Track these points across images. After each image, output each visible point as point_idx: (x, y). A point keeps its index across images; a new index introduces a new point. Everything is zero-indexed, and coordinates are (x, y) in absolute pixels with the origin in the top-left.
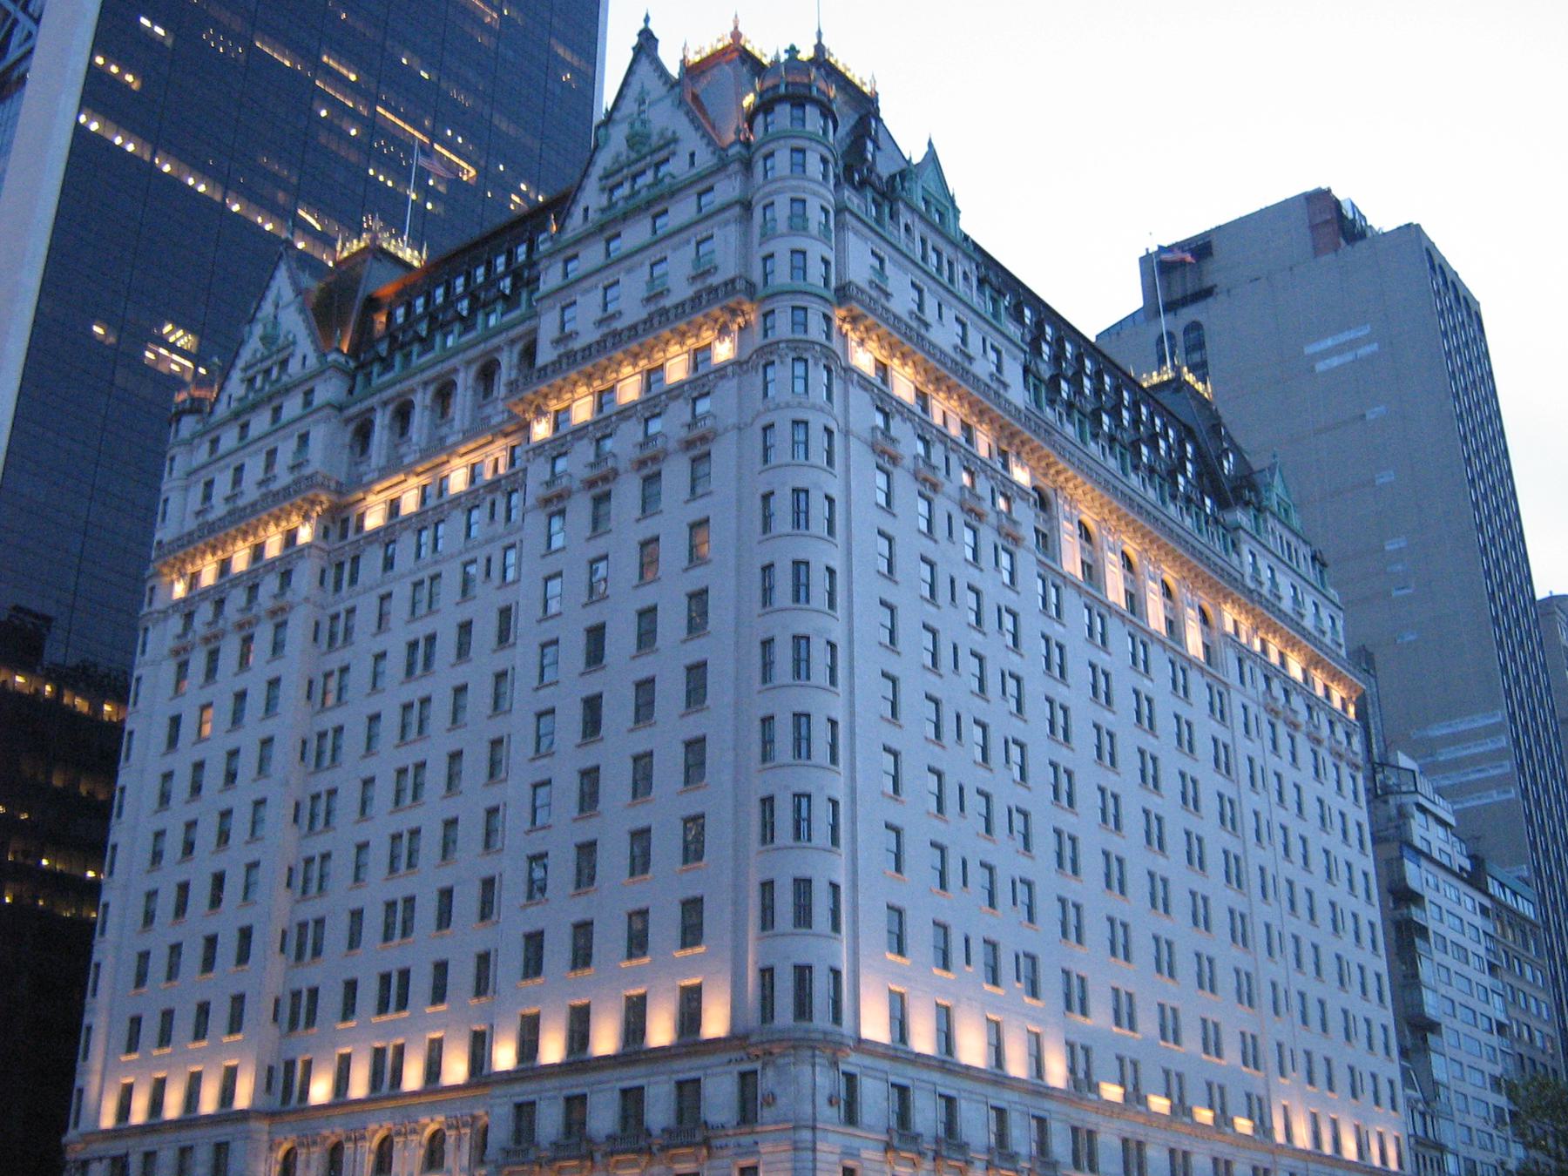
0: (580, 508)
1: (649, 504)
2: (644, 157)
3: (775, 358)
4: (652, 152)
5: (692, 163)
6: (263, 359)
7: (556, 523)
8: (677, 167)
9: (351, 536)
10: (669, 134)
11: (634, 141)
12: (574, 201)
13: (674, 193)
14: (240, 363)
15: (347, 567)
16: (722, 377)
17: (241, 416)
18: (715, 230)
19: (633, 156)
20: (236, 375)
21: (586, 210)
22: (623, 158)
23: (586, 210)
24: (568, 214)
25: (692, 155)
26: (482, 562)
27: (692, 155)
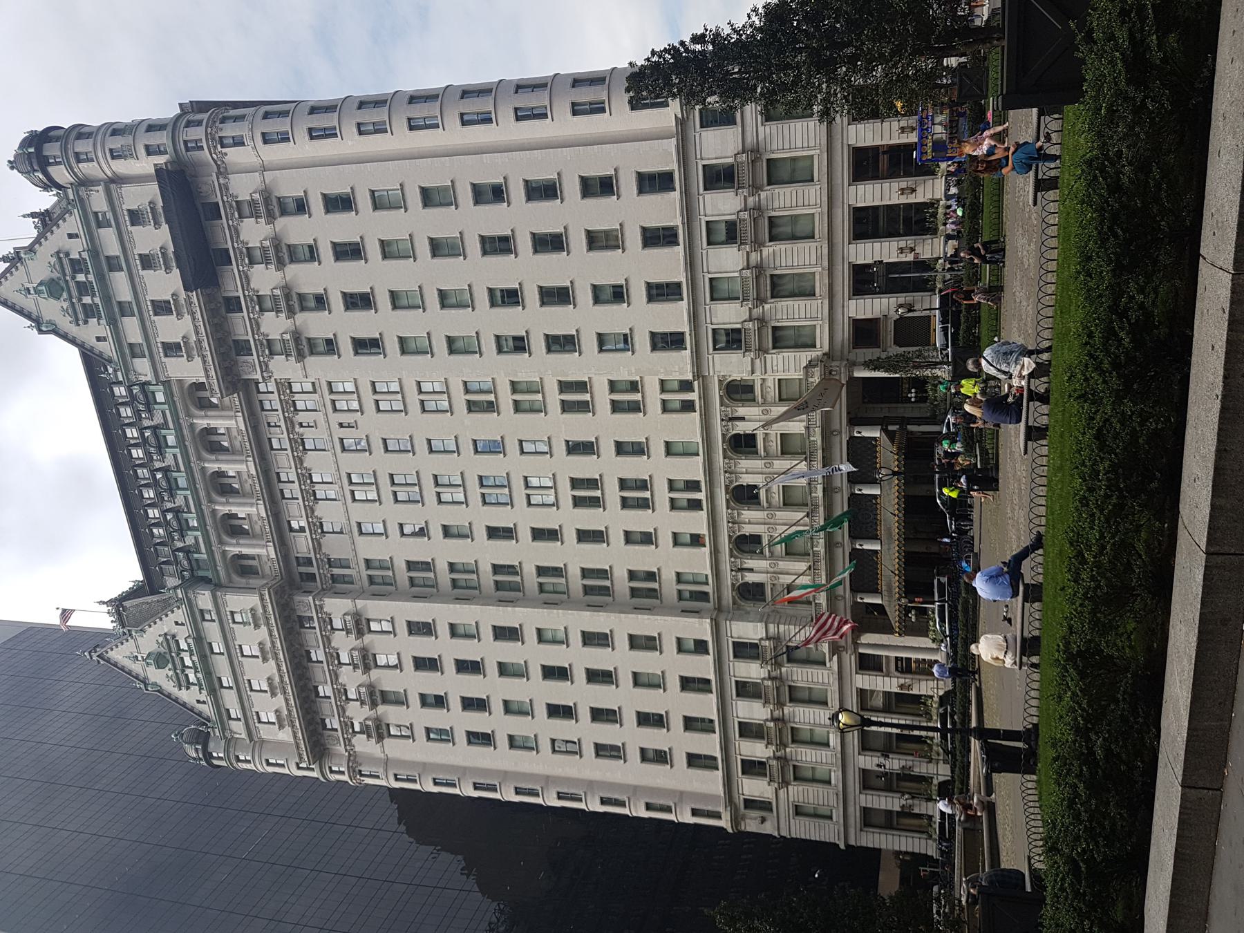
0: (391, 713)
1: (400, 700)
2: (67, 281)
3: (217, 136)
4: (65, 275)
5: (76, 236)
6: (175, 669)
7: (374, 626)
8: (77, 248)
9: (314, 570)
10: (53, 260)
11: (53, 288)
12: (92, 350)
13: (94, 251)
14: (175, 691)
15: (336, 571)
16: (227, 189)
17: (213, 686)
18: (124, 207)
19: (65, 295)
20: (184, 695)
21: (99, 339)
22: (65, 305)
23: (99, 339)
24: (101, 355)
25: (71, 236)
26: (343, 433)
27: (71, 236)
